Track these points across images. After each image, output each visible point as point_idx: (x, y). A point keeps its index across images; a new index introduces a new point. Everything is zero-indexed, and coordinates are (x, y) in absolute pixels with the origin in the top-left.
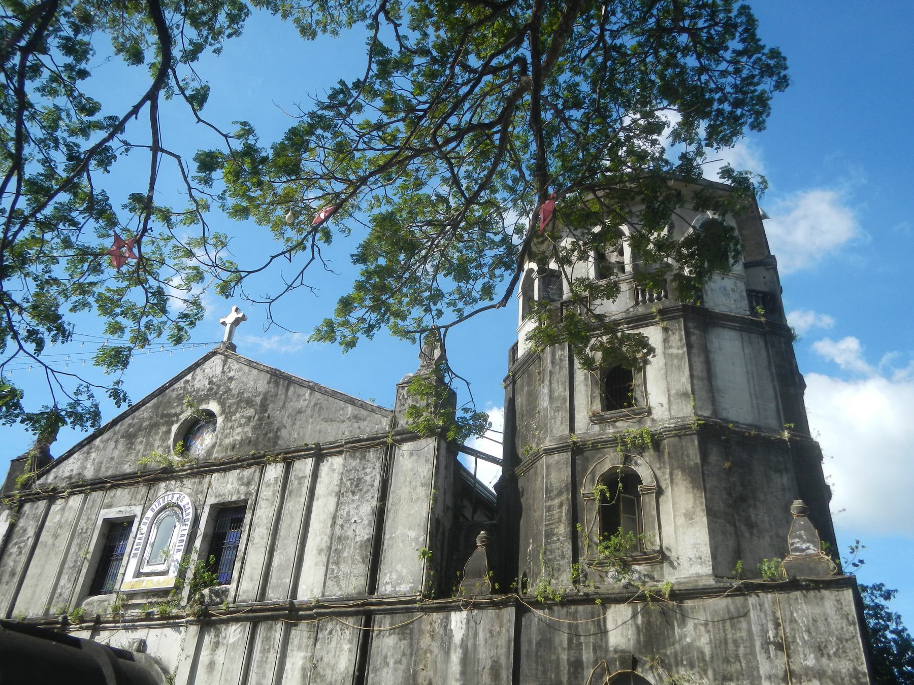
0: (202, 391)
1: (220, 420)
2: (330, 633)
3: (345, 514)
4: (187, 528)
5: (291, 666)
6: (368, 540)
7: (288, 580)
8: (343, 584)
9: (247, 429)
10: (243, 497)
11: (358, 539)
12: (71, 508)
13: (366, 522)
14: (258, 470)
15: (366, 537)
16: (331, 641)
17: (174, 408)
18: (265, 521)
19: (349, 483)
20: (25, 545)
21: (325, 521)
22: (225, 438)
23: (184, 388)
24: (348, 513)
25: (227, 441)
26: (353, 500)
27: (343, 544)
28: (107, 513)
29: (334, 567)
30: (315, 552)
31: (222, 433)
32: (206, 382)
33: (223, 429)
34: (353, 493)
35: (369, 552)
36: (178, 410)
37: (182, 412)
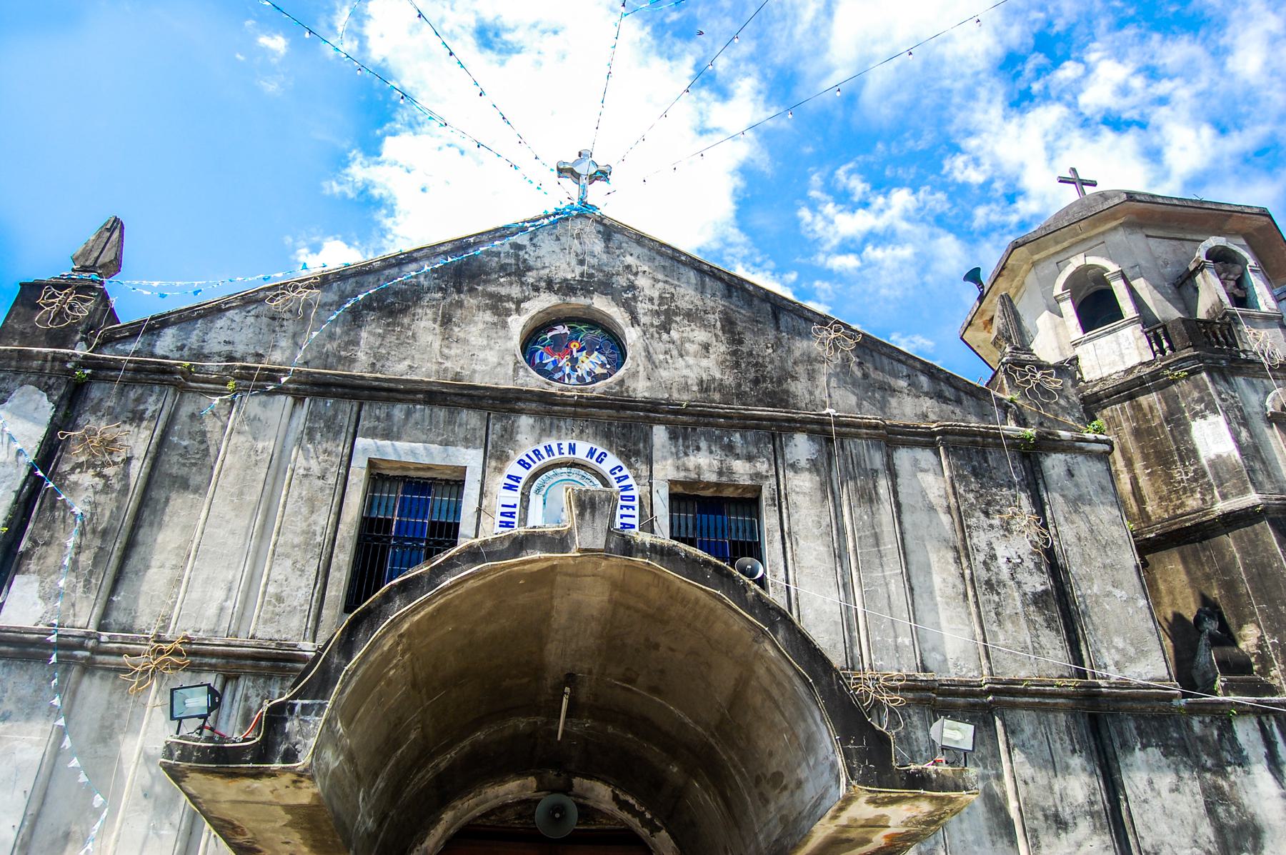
1: (632, 336)
3: (983, 546)
4: (636, 513)
6: (1045, 592)
9: (705, 363)
13: (1032, 565)
15: (1040, 588)
17: (502, 285)
19: (971, 496)
23: (517, 257)
24: (990, 544)
26: (991, 526)
27: (998, 594)
29: (995, 628)
31: (649, 357)
34: (987, 514)
36: (515, 291)
37: (527, 299)
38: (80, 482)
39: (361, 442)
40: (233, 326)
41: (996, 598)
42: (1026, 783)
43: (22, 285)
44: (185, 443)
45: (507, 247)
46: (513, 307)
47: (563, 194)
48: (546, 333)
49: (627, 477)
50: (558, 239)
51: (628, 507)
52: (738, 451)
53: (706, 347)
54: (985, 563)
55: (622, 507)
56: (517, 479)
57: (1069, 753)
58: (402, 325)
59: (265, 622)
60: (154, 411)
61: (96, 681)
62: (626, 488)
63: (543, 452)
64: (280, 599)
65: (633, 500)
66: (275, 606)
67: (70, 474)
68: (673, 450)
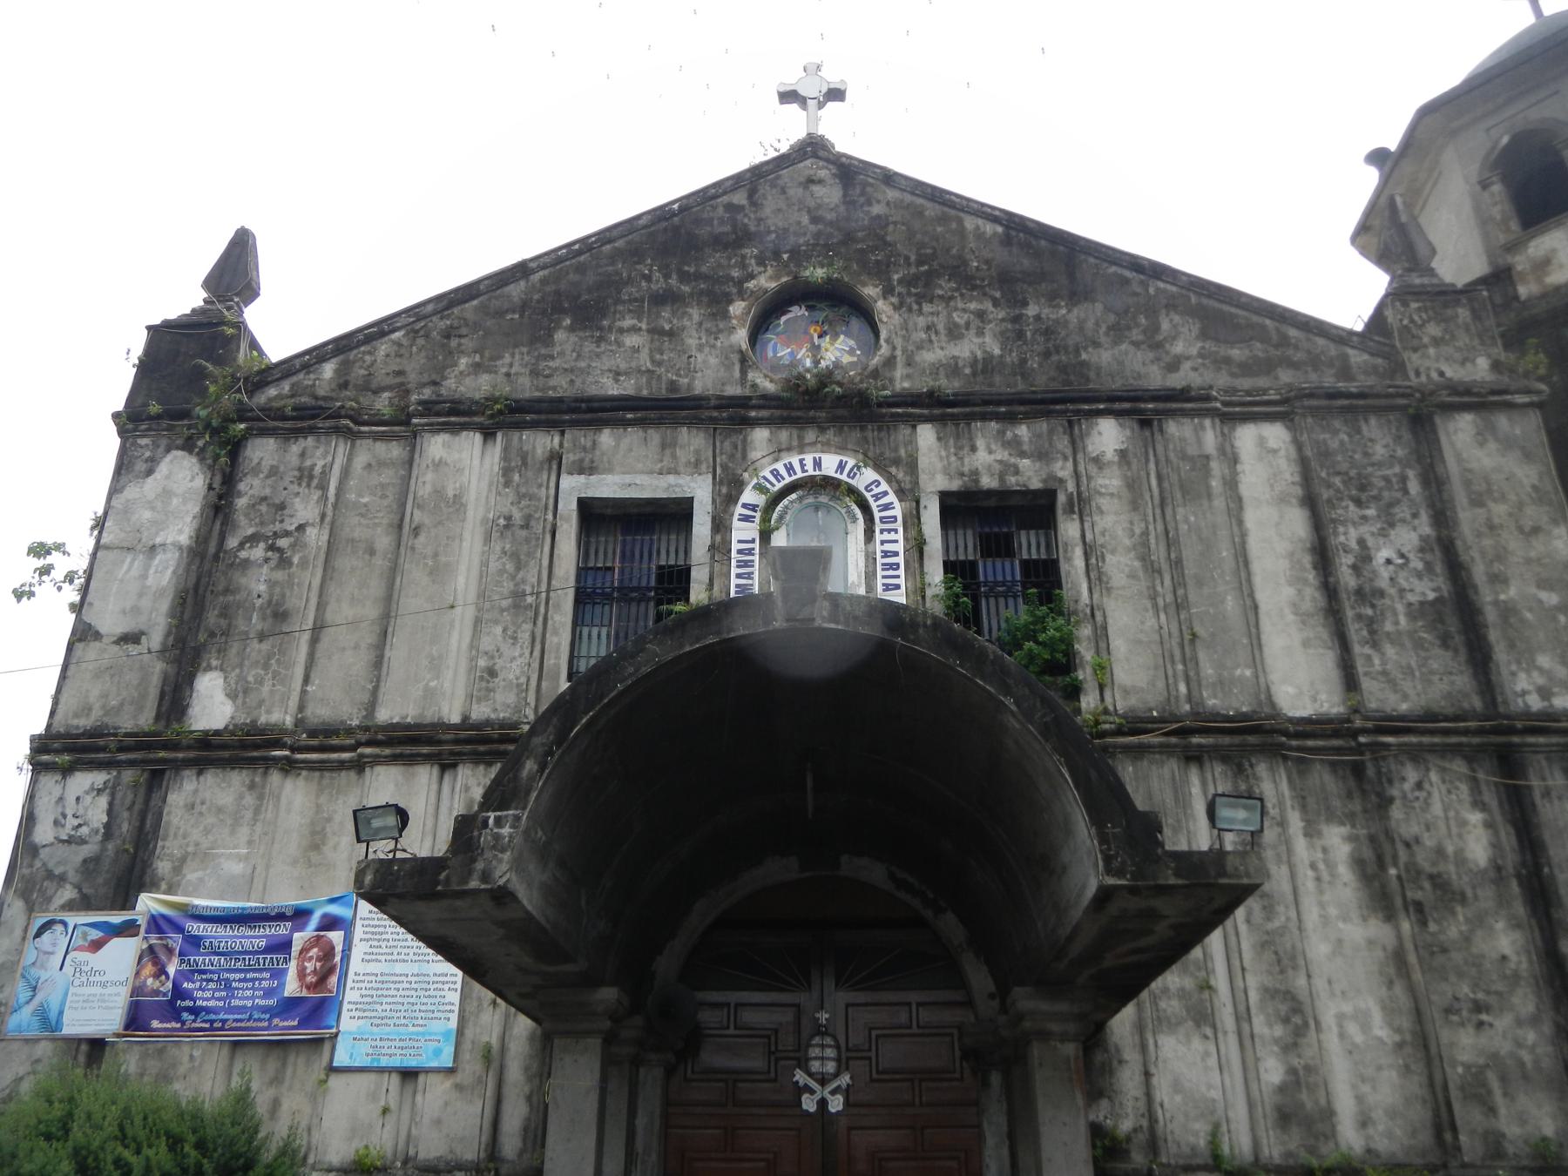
0: (796, 234)
1: (883, 308)
2: (1419, 786)
3: (1354, 545)
4: (900, 536)
5: (1320, 855)
6: (1439, 600)
7: (1248, 673)
8: (1407, 686)
10: (1036, 484)
11: (1411, 598)
12: (438, 465)
13: (1420, 565)
14: (1061, 429)
15: (1431, 596)
16: (1427, 804)
18: (1127, 542)
19: (1337, 481)
20: (293, 546)
21: (1291, 554)
22: (920, 347)
24: (1361, 542)
25: (929, 357)
26: (1364, 518)
27: (1373, 606)
28: (587, 486)
29: (1367, 650)
30: (1291, 617)
31: (906, 339)
32: (805, 220)
33: (905, 326)
34: (1359, 503)
35: (1453, 625)
38: (252, 558)
39: (567, 482)
40: (403, 351)
41: (1369, 612)
42: (1408, 845)
43: (149, 328)
44: (365, 500)
45: (721, 210)
46: (734, 290)
47: (789, 128)
48: (778, 318)
49: (885, 493)
50: (783, 191)
51: (889, 531)
52: (1026, 447)
53: (981, 315)
54: (1355, 567)
55: (882, 531)
56: (754, 508)
57: (1467, 805)
58: (601, 329)
59: (479, 700)
60: (324, 466)
61: (301, 782)
62: (887, 507)
63: (783, 472)
64: (492, 673)
65: (896, 521)
66: (488, 682)
67: (238, 550)
68: (943, 453)
